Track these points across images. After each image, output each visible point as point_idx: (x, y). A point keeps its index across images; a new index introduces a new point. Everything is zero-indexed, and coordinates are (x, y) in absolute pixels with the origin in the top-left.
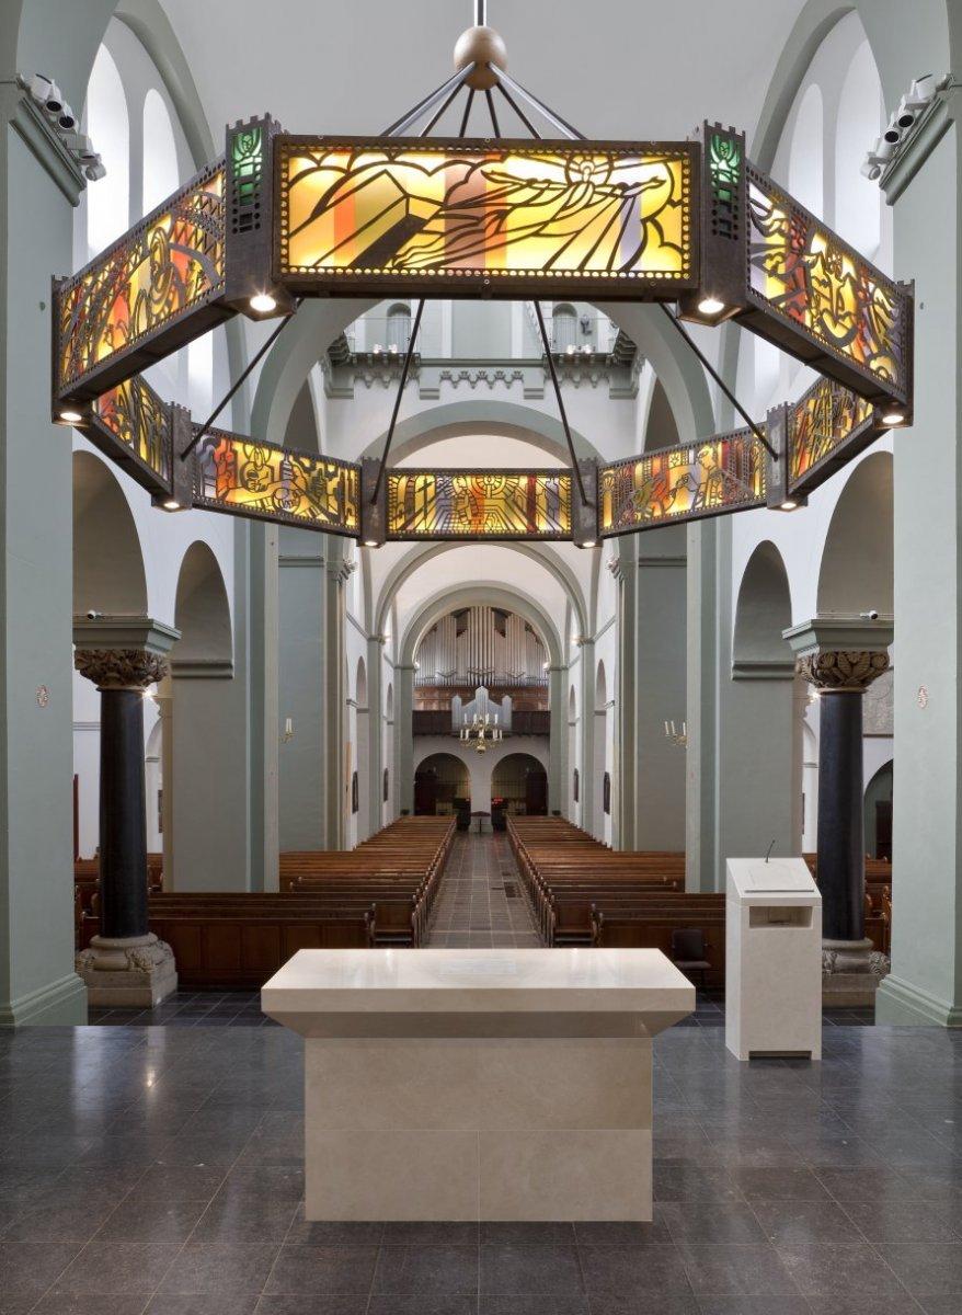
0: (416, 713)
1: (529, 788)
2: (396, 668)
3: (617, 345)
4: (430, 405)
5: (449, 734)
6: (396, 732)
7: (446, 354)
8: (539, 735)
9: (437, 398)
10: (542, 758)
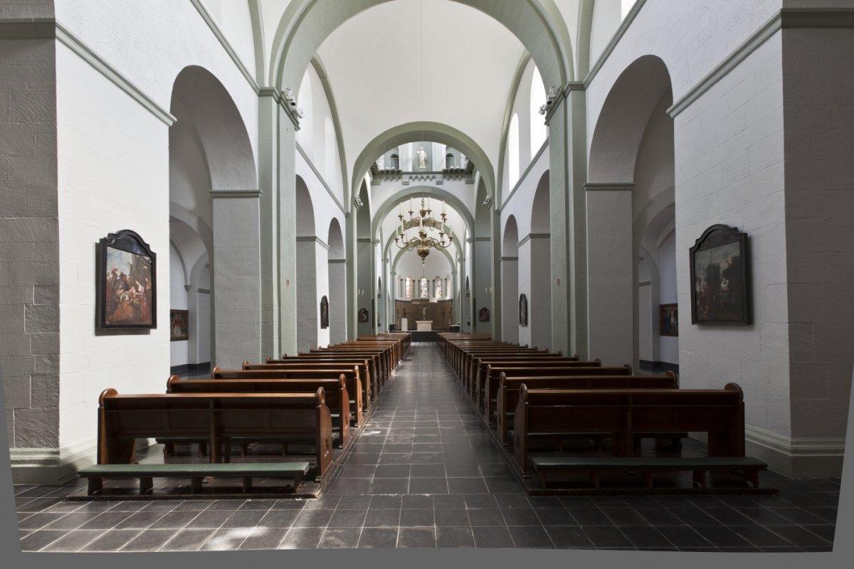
3: (468, 166)
4: (407, 187)
7: (410, 170)
9: (408, 185)
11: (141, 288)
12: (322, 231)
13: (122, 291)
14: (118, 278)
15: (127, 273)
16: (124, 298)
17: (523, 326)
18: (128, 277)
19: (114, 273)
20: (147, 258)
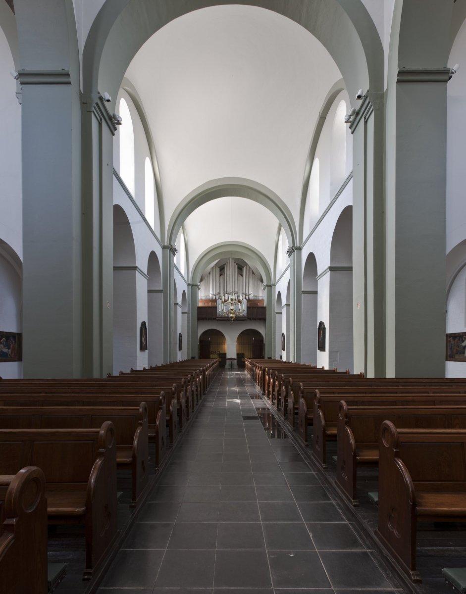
0: (199, 308)
1: (255, 345)
2: (188, 285)
5: (215, 319)
6: (188, 317)
8: (260, 319)
10: (262, 331)
12: (142, 262)
17: (321, 351)
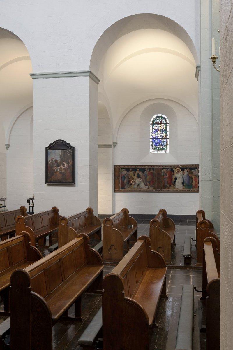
11: (66, 165)
13: (56, 167)
14: (54, 162)
15: (58, 159)
16: (57, 170)
18: (59, 161)
19: (52, 160)
20: (70, 150)
